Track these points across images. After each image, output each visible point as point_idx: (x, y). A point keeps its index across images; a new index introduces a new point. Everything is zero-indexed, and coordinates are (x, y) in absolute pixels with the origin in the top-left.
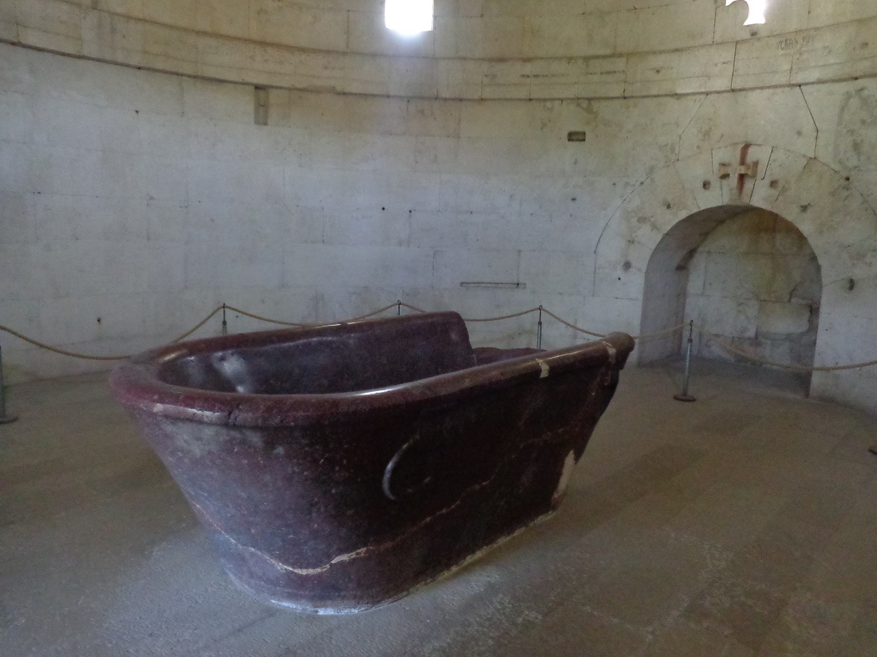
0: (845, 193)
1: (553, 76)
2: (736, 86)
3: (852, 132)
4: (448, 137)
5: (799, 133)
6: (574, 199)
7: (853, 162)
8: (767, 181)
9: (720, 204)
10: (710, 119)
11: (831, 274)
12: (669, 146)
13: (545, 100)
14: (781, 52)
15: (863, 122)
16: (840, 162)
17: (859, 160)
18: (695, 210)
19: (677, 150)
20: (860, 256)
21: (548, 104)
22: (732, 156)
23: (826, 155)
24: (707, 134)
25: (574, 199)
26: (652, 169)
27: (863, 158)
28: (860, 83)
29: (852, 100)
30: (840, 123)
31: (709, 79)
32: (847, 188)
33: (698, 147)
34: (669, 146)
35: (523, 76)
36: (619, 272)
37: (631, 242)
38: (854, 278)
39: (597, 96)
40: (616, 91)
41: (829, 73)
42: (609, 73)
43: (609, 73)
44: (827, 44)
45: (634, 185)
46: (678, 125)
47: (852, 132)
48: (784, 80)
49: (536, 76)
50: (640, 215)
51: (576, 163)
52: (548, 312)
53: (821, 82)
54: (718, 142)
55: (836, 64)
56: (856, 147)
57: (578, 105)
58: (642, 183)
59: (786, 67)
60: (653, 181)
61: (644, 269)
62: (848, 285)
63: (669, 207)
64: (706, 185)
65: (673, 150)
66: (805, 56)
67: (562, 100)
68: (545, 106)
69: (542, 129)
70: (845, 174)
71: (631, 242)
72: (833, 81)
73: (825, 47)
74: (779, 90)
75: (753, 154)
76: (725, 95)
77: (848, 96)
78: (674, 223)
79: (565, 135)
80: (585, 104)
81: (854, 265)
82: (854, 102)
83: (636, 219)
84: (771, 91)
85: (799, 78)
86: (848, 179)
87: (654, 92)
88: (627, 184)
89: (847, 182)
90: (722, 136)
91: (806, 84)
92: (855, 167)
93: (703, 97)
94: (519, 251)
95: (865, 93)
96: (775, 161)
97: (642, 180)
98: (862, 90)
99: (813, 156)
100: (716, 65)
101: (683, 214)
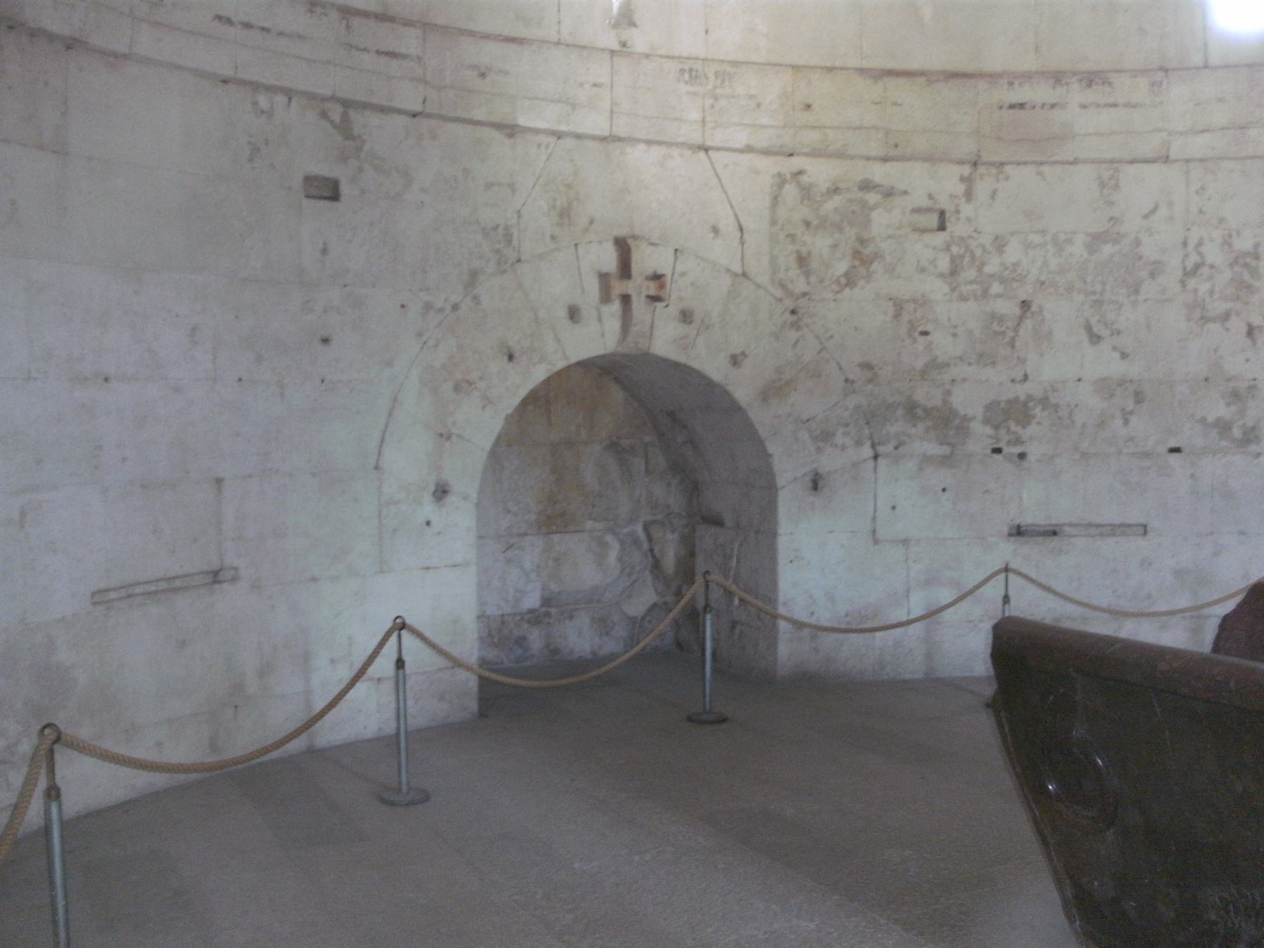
0: (793, 335)
1: (281, 34)
2: (621, 129)
3: (792, 237)
4: (41, 148)
5: (715, 230)
6: (325, 341)
7: (800, 286)
8: (673, 310)
9: (602, 352)
10: (569, 186)
11: (788, 470)
12: (500, 230)
13: (256, 87)
14: (684, 88)
15: (807, 224)
16: (783, 286)
17: (808, 283)
18: (561, 364)
19: (515, 242)
20: (826, 436)
21: (263, 101)
22: (608, 259)
23: (760, 269)
24: (565, 214)
25: (325, 341)
26: (474, 274)
27: (813, 279)
28: (797, 163)
29: (787, 186)
30: (773, 222)
31: (574, 109)
32: (796, 326)
33: (553, 237)
34: (500, 230)
35: (219, 18)
36: (428, 509)
37: (445, 436)
38: (820, 471)
39: (374, 100)
40: (409, 98)
41: (762, 140)
42: (392, 55)
43: (392, 55)
44: (753, 92)
45: (441, 310)
46: (512, 187)
47: (792, 237)
48: (697, 138)
49: (248, 26)
50: (459, 376)
51: (324, 251)
52: (1020, 574)
53: (749, 149)
54: (586, 230)
55: (772, 127)
56: (802, 261)
57: (324, 115)
58: (455, 307)
59: (695, 115)
60: (476, 299)
61: (474, 496)
62: (810, 485)
63: (511, 358)
64: (574, 314)
65: (508, 238)
66: (722, 103)
67: (289, 93)
68: (255, 104)
69: (250, 160)
70: (789, 304)
71: (445, 436)
72: (766, 152)
73: (751, 97)
74: (675, 152)
75: (646, 259)
76: (590, 144)
77: (781, 181)
78: (523, 392)
79: (298, 178)
80: (336, 113)
81: (819, 450)
82: (790, 190)
83: (450, 384)
84: (663, 150)
85: (717, 138)
86: (793, 312)
87: (479, 114)
88: (428, 307)
89: (794, 318)
90: (591, 222)
91: (718, 149)
92: (804, 294)
93: (552, 140)
94: (219, 481)
95: (805, 179)
96: (683, 274)
97: (455, 298)
98: (800, 173)
99: (739, 271)
100: (581, 85)
101: (540, 374)
